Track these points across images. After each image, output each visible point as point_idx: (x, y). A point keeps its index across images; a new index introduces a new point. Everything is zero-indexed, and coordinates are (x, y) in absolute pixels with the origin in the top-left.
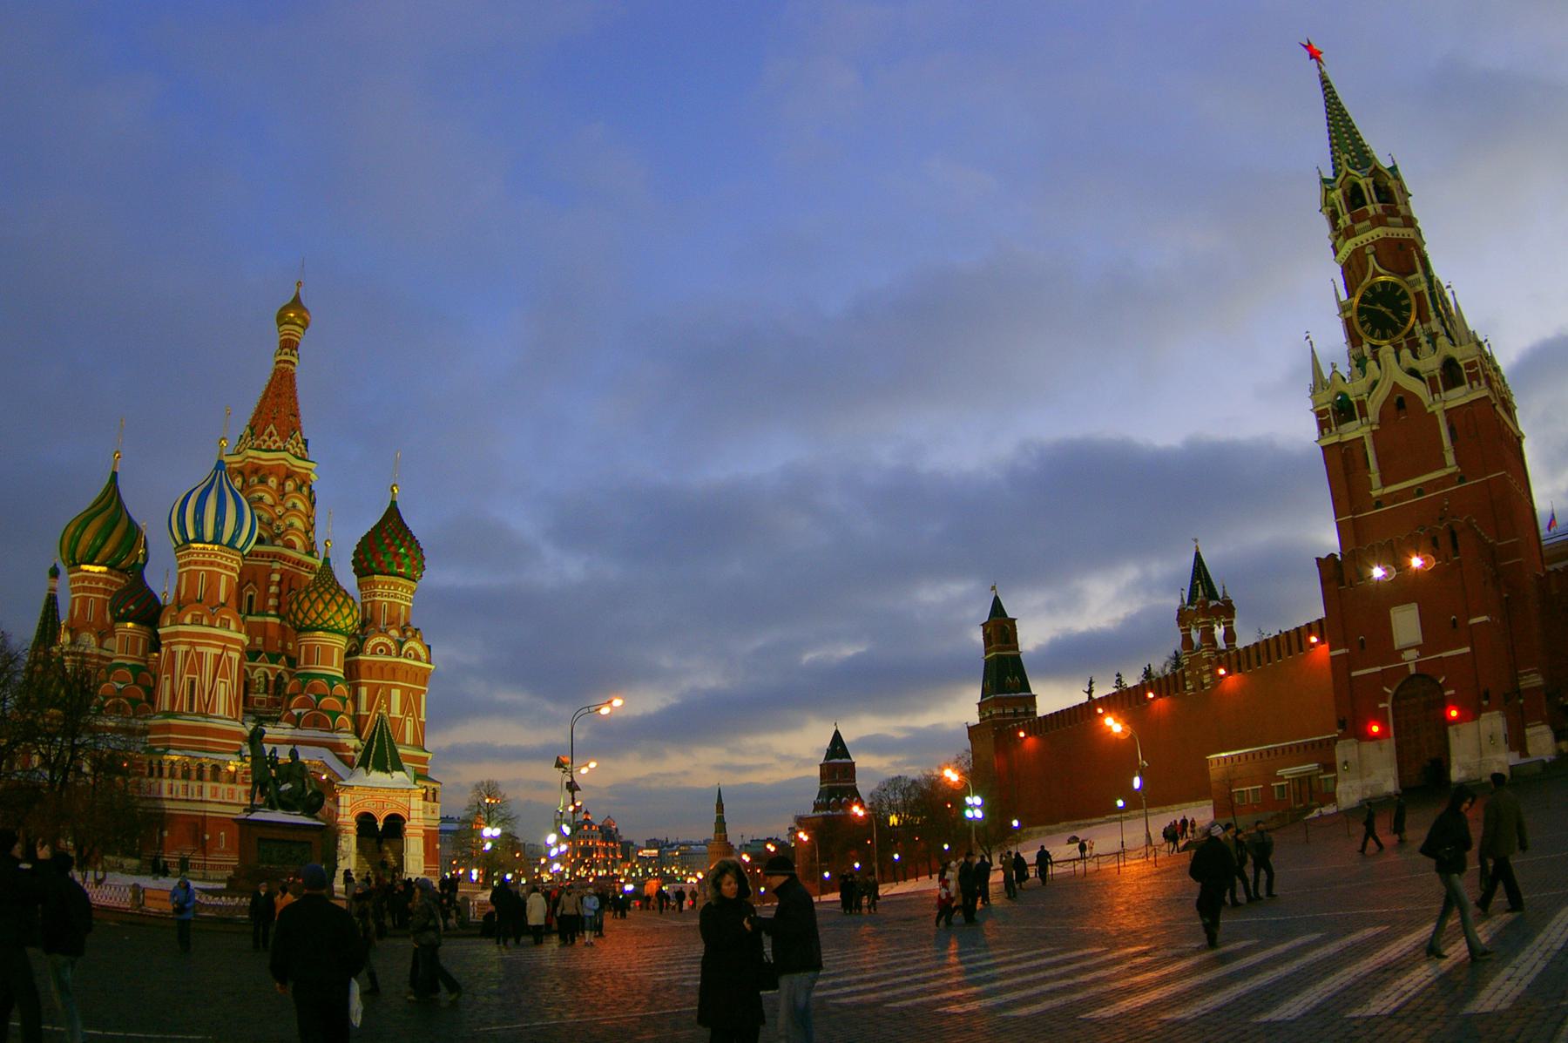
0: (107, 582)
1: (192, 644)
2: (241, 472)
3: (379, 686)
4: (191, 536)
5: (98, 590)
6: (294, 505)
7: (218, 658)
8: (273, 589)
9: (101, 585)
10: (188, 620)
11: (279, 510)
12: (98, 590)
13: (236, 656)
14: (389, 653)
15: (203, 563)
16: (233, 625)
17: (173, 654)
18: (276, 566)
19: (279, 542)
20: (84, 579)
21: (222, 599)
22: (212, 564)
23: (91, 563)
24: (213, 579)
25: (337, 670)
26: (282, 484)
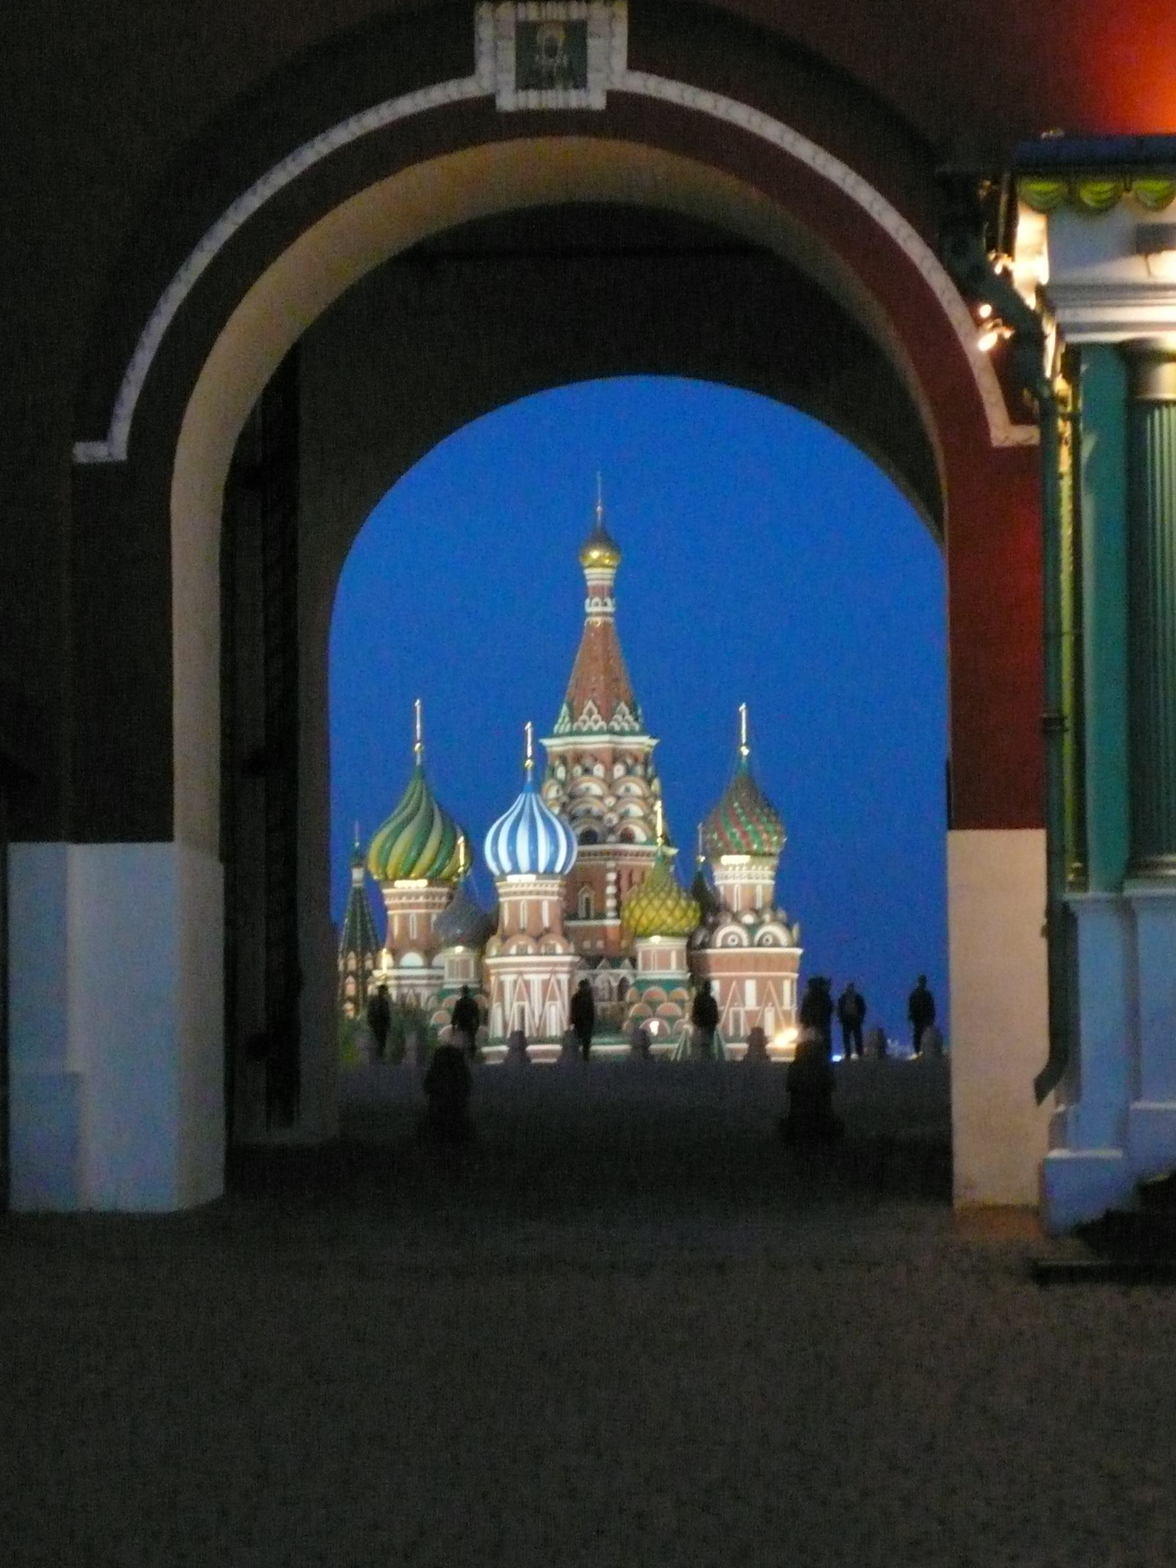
0: (427, 895)
1: (521, 973)
2: (563, 759)
3: (731, 979)
4: (507, 866)
5: (418, 906)
6: (628, 790)
7: (545, 984)
8: (611, 890)
9: (421, 900)
10: (513, 950)
11: (610, 801)
12: (418, 906)
13: (564, 978)
14: (740, 946)
15: (523, 893)
16: (559, 949)
17: (501, 985)
18: (611, 864)
19: (612, 838)
20: (401, 895)
21: (546, 923)
22: (530, 893)
23: (406, 876)
24: (536, 908)
25: (675, 971)
26: (609, 771)
